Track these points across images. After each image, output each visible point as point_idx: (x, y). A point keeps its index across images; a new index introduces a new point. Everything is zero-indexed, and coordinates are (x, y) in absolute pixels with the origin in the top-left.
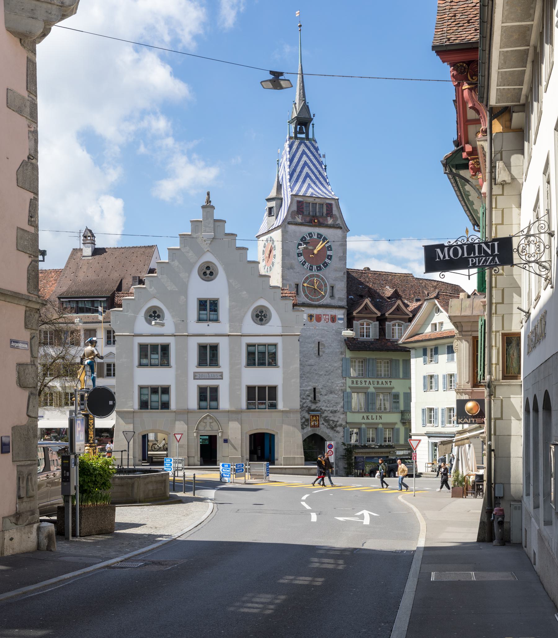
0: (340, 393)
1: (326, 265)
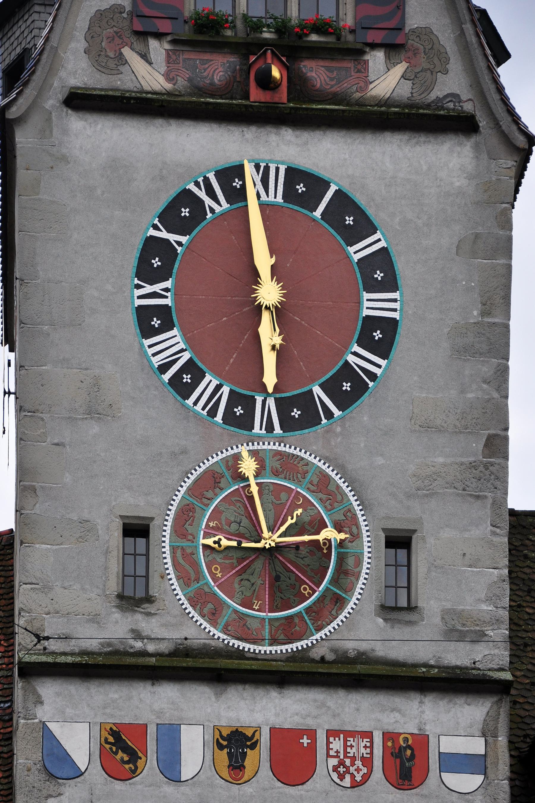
1: (349, 388)
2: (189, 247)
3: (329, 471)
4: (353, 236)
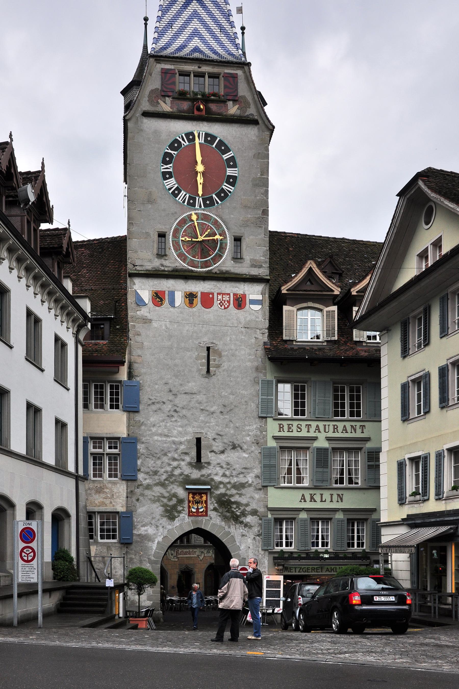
0: (253, 448)
2: (177, 155)
3: (218, 219)
4: (224, 152)
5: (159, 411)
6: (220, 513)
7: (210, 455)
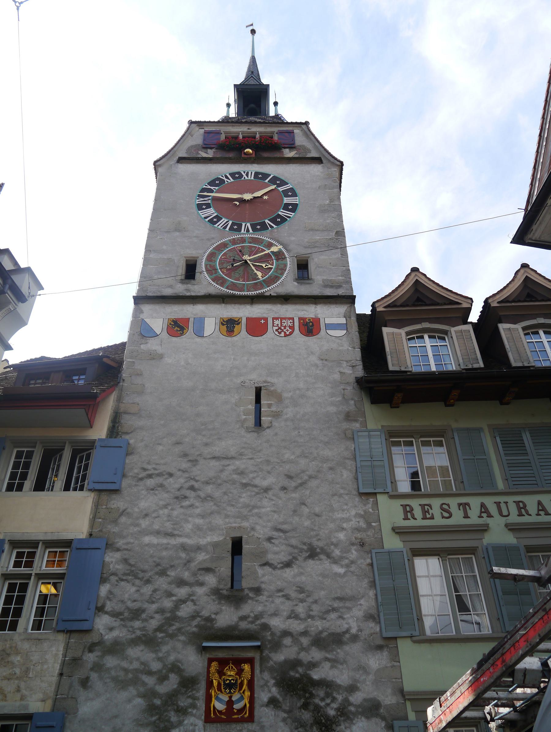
0: (354, 554)
1: (279, 221)
5: (159, 489)
6: (285, 711)
7: (260, 571)
